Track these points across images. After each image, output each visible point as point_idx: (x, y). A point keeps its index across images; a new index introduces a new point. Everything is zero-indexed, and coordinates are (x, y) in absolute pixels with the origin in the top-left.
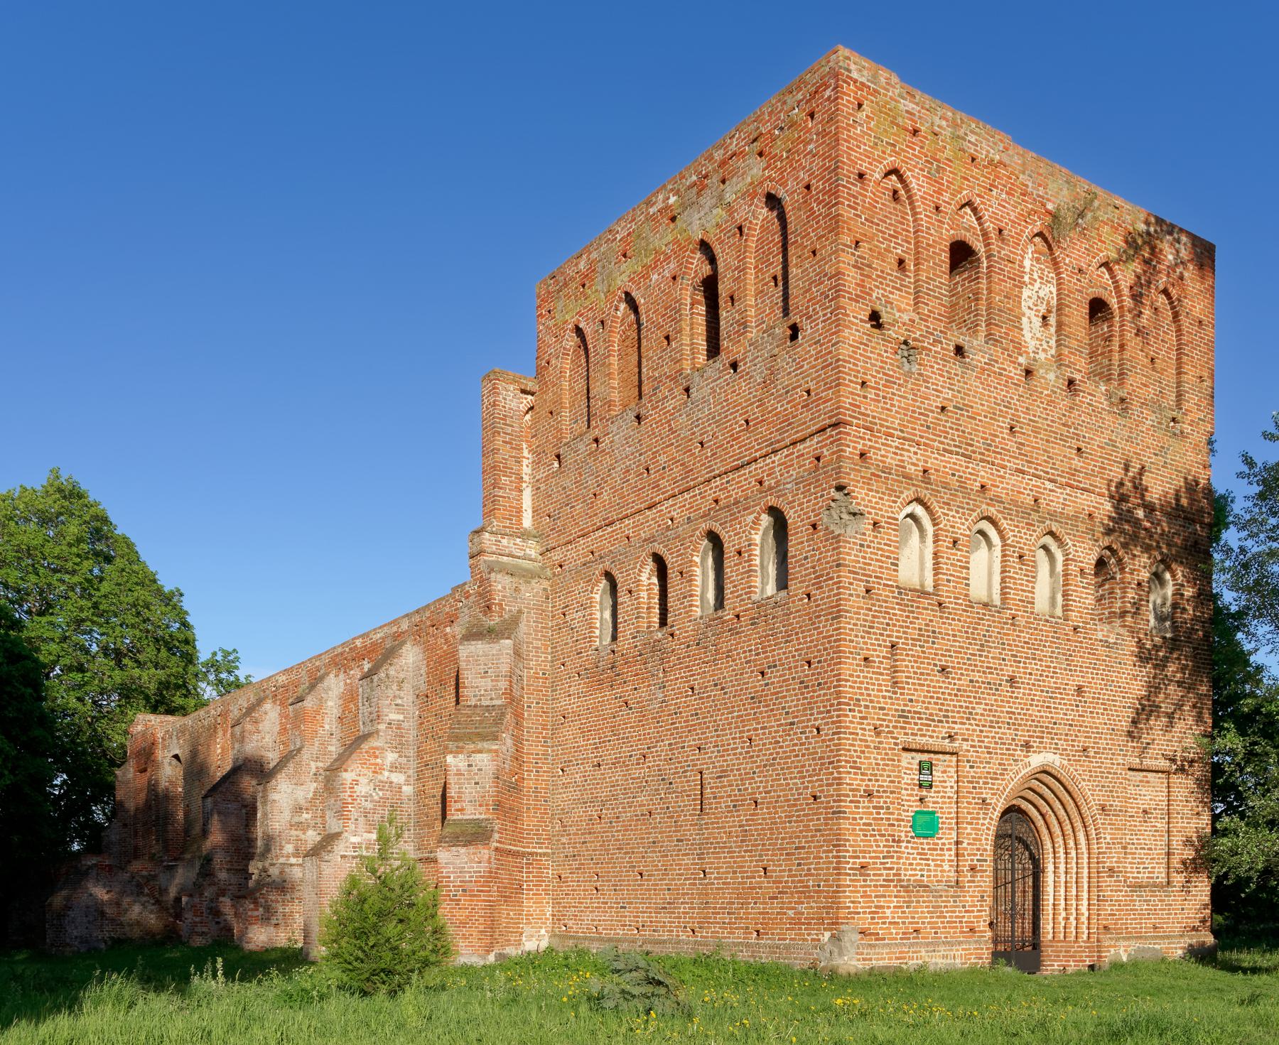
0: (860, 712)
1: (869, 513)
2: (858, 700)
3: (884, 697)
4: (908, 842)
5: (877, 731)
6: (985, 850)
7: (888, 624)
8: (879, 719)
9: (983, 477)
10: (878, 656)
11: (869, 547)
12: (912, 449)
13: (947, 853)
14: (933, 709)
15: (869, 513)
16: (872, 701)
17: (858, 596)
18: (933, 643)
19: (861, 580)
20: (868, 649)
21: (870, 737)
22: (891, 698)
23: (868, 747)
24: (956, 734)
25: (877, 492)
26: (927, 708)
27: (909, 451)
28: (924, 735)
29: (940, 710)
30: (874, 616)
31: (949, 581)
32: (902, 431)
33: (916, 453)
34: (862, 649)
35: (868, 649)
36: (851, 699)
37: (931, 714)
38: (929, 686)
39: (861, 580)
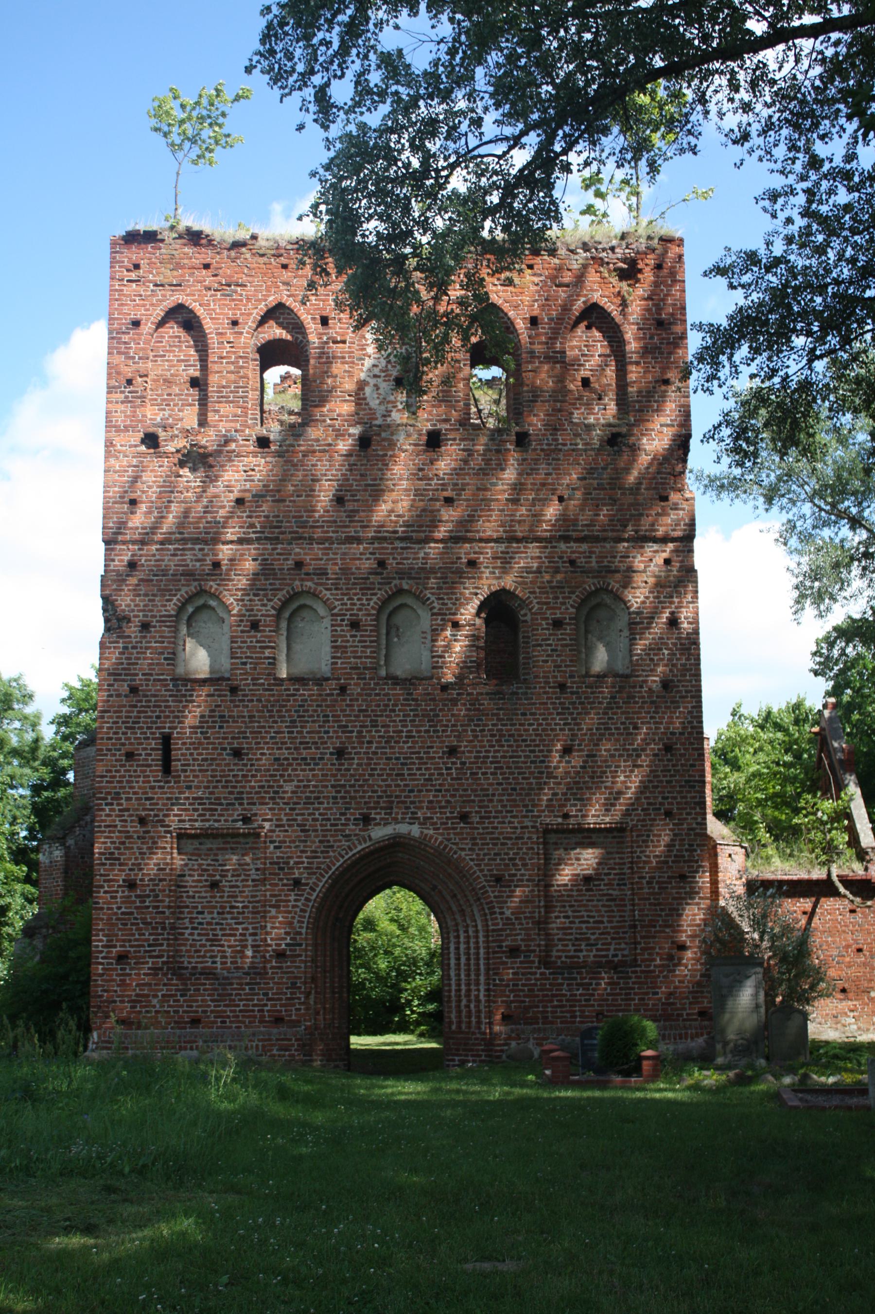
0: (118, 804)
1: (135, 616)
2: (118, 793)
3: (152, 788)
4: (193, 928)
5: (142, 821)
6: (300, 933)
7: (158, 717)
8: (144, 810)
9: (299, 554)
10: (145, 749)
11: (133, 648)
12: (197, 547)
13: (250, 938)
14: (220, 792)
15: (135, 616)
16: (135, 793)
17: (118, 696)
18: (221, 727)
19: (124, 680)
20: (131, 744)
21: (134, 828)
22: (161, 787)
23: (131, 837)
24: (256, 815)
25: (146, 595)
26: (211, 793)
27: (193, 549)
28: (208, 820)
29: (231, 793)
30: (139, 712)
31: (245, 664)
32: (180, 533)
33: (201, 550)
34: (123, 744)
35: (131, 744)
36: (109, 793)
37: (219, 799)
38: (213, 770)
39: (124, 680)
